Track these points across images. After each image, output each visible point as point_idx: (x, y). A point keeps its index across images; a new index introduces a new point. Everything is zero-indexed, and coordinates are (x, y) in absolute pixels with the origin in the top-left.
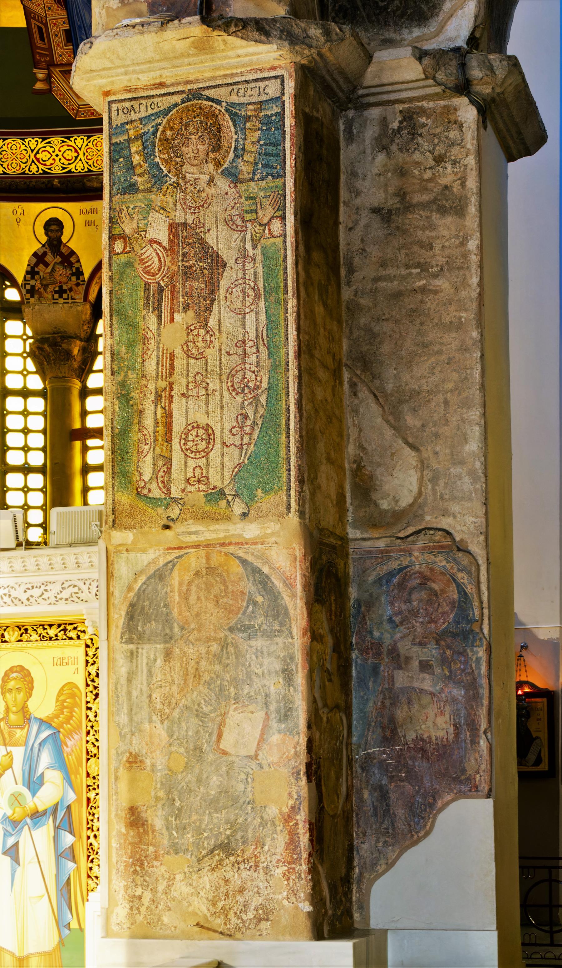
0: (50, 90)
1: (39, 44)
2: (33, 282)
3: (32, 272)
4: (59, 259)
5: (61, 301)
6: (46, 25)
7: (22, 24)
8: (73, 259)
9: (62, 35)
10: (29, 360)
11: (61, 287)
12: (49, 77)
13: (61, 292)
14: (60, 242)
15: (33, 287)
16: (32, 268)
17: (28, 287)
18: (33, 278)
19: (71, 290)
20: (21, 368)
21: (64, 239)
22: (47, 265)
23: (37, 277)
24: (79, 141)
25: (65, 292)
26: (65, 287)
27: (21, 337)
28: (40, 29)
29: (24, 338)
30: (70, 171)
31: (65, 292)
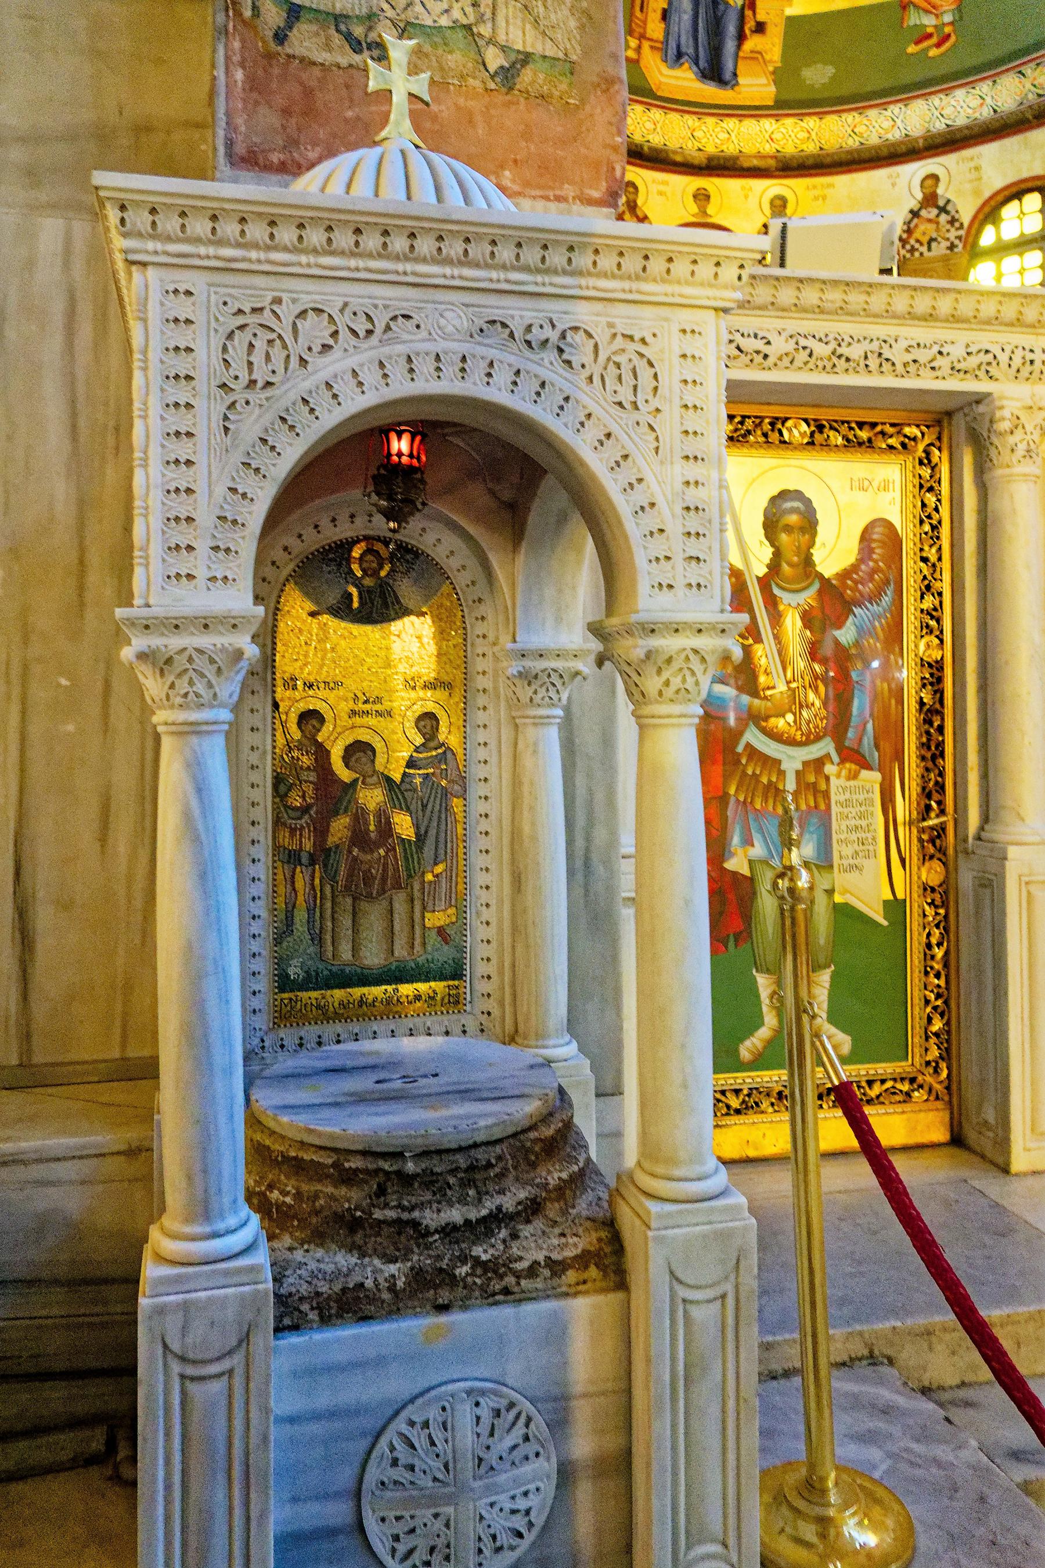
1: (638, 13)
9: (659, 14)
12: (639, 47)
14: (635, 202)
21: (639, 202)
24: (656, 114)
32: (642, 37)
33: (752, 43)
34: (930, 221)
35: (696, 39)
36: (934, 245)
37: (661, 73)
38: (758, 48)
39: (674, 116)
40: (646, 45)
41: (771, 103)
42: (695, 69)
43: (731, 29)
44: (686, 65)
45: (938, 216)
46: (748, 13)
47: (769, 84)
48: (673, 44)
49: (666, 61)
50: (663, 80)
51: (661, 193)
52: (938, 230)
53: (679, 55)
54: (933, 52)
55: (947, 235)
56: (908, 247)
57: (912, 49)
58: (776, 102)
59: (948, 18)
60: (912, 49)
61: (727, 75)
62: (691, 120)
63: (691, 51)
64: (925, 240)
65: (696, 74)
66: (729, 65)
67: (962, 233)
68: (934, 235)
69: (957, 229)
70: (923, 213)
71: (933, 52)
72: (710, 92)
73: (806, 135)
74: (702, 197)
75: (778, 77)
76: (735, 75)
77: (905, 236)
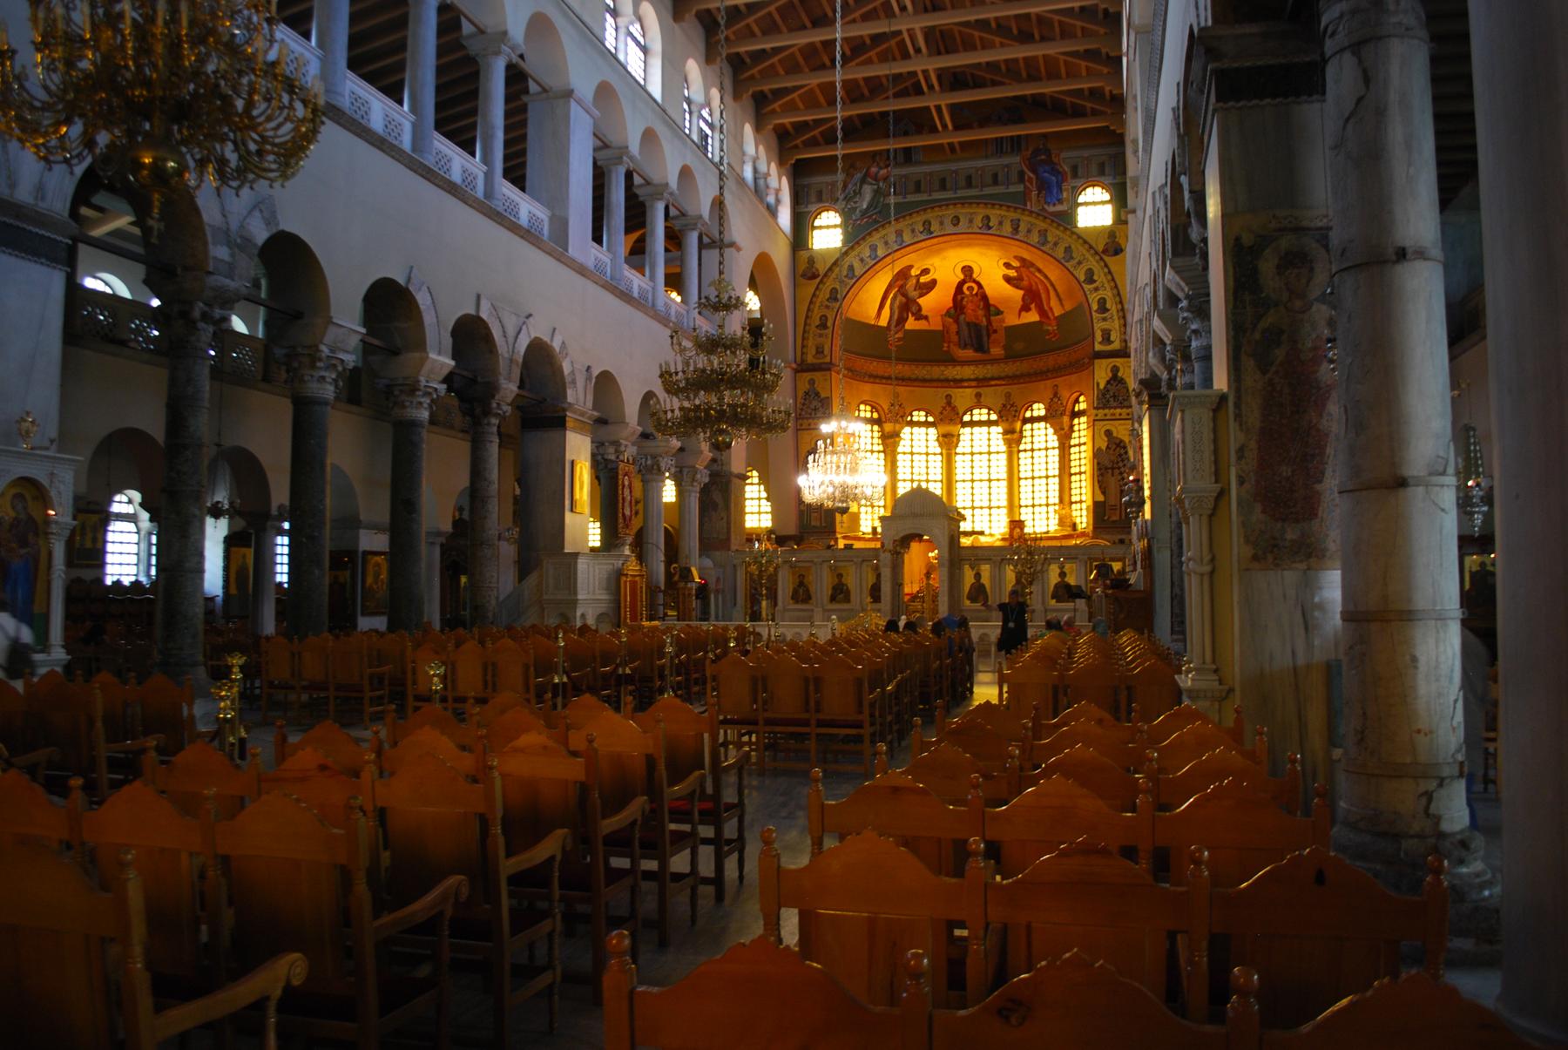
3: (941, 413)
12: (948, 347)
24: (958, 368)
33: (994, 336)
39: (966, 368)
40: (952, 345)
43: (984, 333)
61: (986, 348)
62: (972, 368)
72: (978, 355)
74: (978, 395)
75: (1005, 348)
76: (989, 349)
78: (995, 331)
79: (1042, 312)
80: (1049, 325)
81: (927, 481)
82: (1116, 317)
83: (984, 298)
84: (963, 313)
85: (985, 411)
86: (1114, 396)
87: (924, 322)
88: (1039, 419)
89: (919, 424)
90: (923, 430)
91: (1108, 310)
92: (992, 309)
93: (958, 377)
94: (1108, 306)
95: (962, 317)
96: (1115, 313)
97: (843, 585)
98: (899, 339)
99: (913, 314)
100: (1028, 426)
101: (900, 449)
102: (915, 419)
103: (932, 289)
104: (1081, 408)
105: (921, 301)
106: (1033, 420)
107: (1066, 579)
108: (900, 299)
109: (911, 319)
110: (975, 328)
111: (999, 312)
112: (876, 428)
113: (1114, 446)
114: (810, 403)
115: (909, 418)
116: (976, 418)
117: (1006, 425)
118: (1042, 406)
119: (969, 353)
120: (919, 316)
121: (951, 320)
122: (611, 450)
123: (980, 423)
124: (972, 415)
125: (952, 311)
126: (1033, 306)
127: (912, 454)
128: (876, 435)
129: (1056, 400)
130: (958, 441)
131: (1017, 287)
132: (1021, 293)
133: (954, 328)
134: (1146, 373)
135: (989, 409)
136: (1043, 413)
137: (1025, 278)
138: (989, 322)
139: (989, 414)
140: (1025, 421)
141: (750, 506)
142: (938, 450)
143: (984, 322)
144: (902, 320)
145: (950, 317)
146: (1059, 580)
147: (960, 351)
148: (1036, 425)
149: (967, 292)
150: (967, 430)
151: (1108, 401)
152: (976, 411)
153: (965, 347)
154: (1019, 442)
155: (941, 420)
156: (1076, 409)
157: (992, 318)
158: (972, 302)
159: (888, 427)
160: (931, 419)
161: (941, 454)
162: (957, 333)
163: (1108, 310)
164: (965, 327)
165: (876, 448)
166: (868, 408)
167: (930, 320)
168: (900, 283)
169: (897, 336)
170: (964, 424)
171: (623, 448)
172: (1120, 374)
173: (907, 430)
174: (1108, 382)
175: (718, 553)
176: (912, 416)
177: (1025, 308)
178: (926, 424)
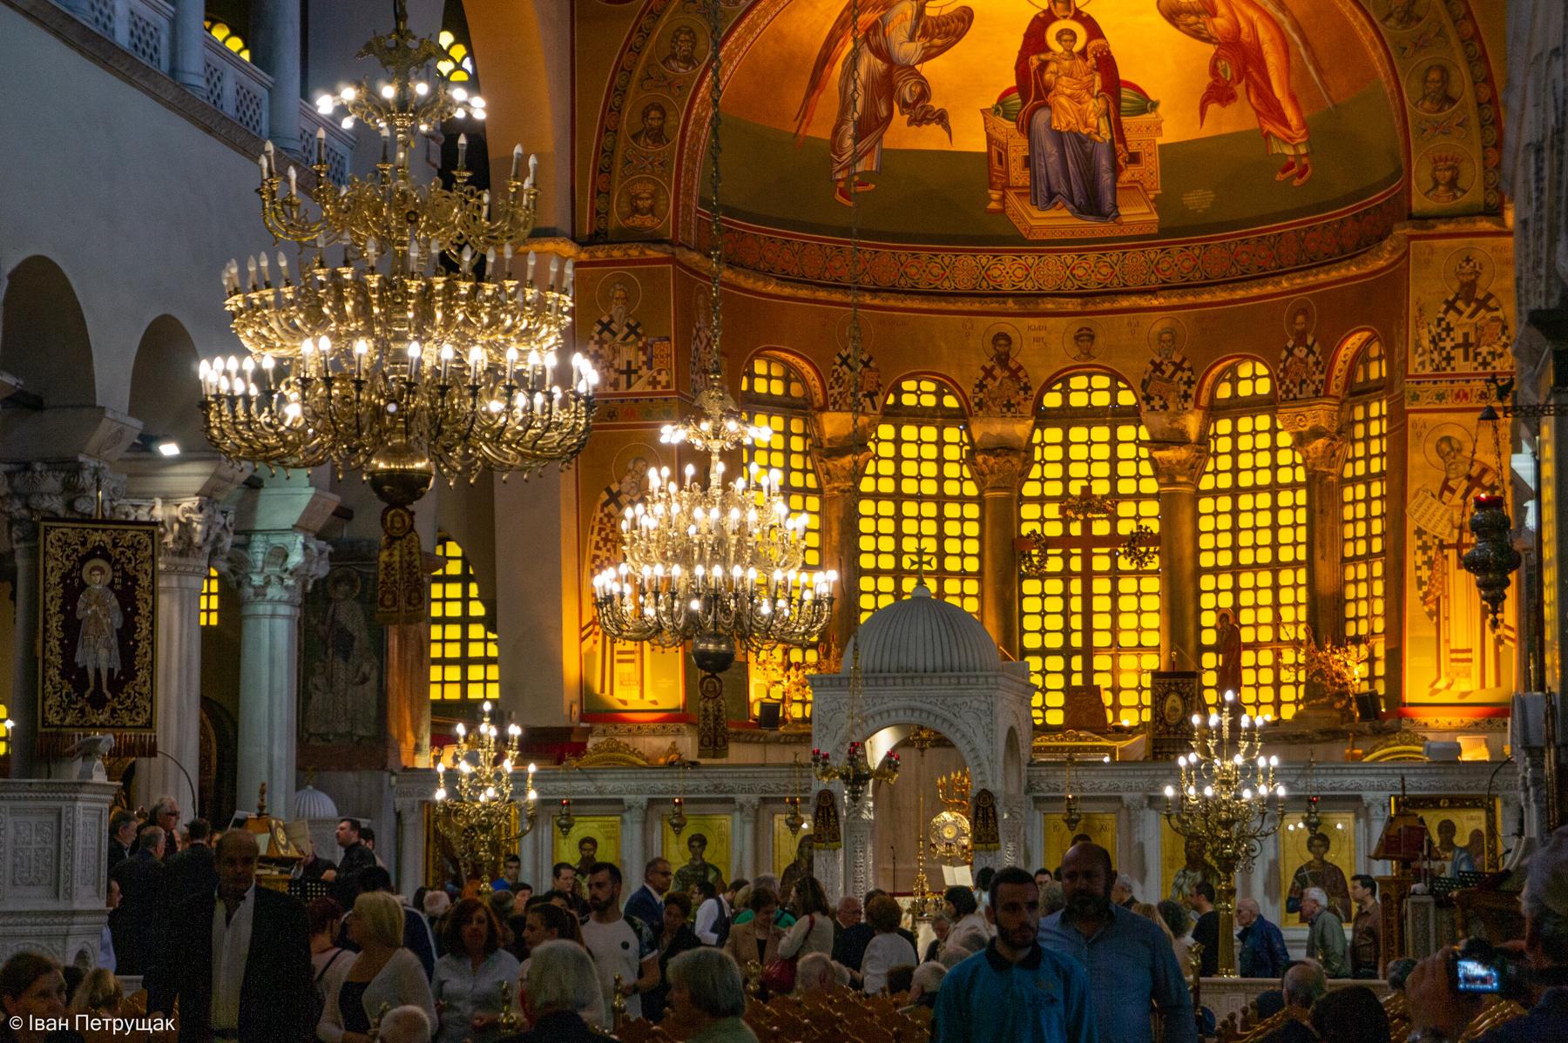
0: (1003, 211)
1: (997, 166)
2: (981, 395)
3: (981, 386)
4: (1007, 374)
5: (1009, 415)
6: (1006, 151)
7: (984, 149)
8: (1021, 374)
9: (1020, 162)
10: (965, 467)
11: (1009, 401)
12: (1004, 197)
13: (1009, 406)
14: (1007, 355)
15: (981, 400)
16: (981, 382)
17: (977, 400)
18: (981, 391)
19: (1019, 404)
20: (957, 475)
21: (1012, 355)
22: (995, 379)
23: (985, 390)
25: (1013, 405)
26: (1013, 402)
27: (957, 444)
28: (1000, 155)
29: (960, 444)
30: (1020, 289)
31: (1013, 405)
32: (1006, 187)
34: (1301, 360)
35: (1068, 180)
36: (1304, 386)
37: (1032, 218)
38: (1137, 177)
39: (1051, 258)
40: (1011, 194)
41: (1155, 230)
42: (1071, 206)
43: (1104, 163)
44: (1060, 204)
45: (1307, 356)
46: (1119, 146)
47: (1151, 213)
48: (1042, 186)
49: (1035, 203)
50: (1033, 223)
51: (1037, 340)
52: (1307, 372)
53: (1051, 196)
54: (1297, 182)
55: (1314, 378)
56: (1284, 387)
57: (1279, 177)
58: (1160, 230)
59: (1302, 150)
60: (1279, 177)
61: (1107, 208)
62: (1068, 258)
63: (1063, 189)
64: (1298, 380)
65: (1072, 211)
66: (1109, 197)
67: (1323, 377)
68: (1304, 377)
69: (1322, 372)
70: (1296, 351)
71: (1297, 182)
73: (1192, 263)
74: (1085, 337)
75: (1159, 204)
76: (1115, 207)
77: (1281, 375)
78: (1135, 158)
79: (1270, 108)
80: (1288, 141)
81: (942, 574)
82: (1474, 122)
83: (1106, 64)
84: (1047, 106)
85: (1102, 381)
86: (1466, 345)
87: (935, 129)
88: (1254, 406)
89: (920, 416)
90: (929, 433)
91: (1452, 101)
92: (1126, 94)
93: (1028, 286)
94: (1454, 90)
95: (1041, 117)
96: (1472, 113)
97: (706, 867)
98: (865, 179)
99: (905, 105)
100: (1224, 426)
101: (867, 485)
102: (909, 400)
103: (959, 36)
104: (1374, 374)
105: (926, 69)
106: (1238, 407)
107: (1330, 857)
108: (869, 63)
109: (899, 119)
110: (1075, 144)
111: (1145, 105)
112: (797, 425)
113: (1465, 484)
114: (616, 352)
115: (891, 400)
116: (1078, 400)
117: (1162, 421)
118: (1262, 370)
119: (1058, 220)
120: (924, 112)
121: (1011, 125)
122: (52, 483)
123: (1090, 416)
124: (1066, 392)
125: (1016, 99)
126: (1240, 89)
127: (898, 497)
128: (797, 444)
129: (1301, 352)
130: (1029, 462)
131: (1197, 34)
132: (1211, 49)
133: (1018, 147)
134: (1549, 294)
135: (1115, 377)
136: (1264, 387)
137: (1222, 10)
138: (1118, 130)
139: (1113, 391)
140: (1215, 410)
141: (443, 641)
142: (971, 489)
143: (1105, 134)
144: (871, 126)
145: (1006, 116)
146: (1311, 857)
147: (1036, 213)
148: (1245, 424)
149: (1057, 47)
150: (1054, 434)
151: (1449, 359)
152: (1078, 382)
153: (1050, 199)
154: (1195, 470)
155: (980, 405)
156: (1360, 378)
157: (1126, 121)
158: (1070, 75)
159: (834, 424)
160: (950, 402)
161: (979, 500)
162: (1028, 162)
163: (1452, 101)
164: (1050, 148)
165: (796, 480)
166: (776, 371)
167: (952, 121)
168: (867, 18)
169: (860, 168)
170: (1044, 418)
171: (87, 478)
172: (1482, 282)
173: (886, 431)
174: (1451, 306)
175: (351, 777)
176: (899, 392)
177: (1219, 93)
178: (938, 417)
